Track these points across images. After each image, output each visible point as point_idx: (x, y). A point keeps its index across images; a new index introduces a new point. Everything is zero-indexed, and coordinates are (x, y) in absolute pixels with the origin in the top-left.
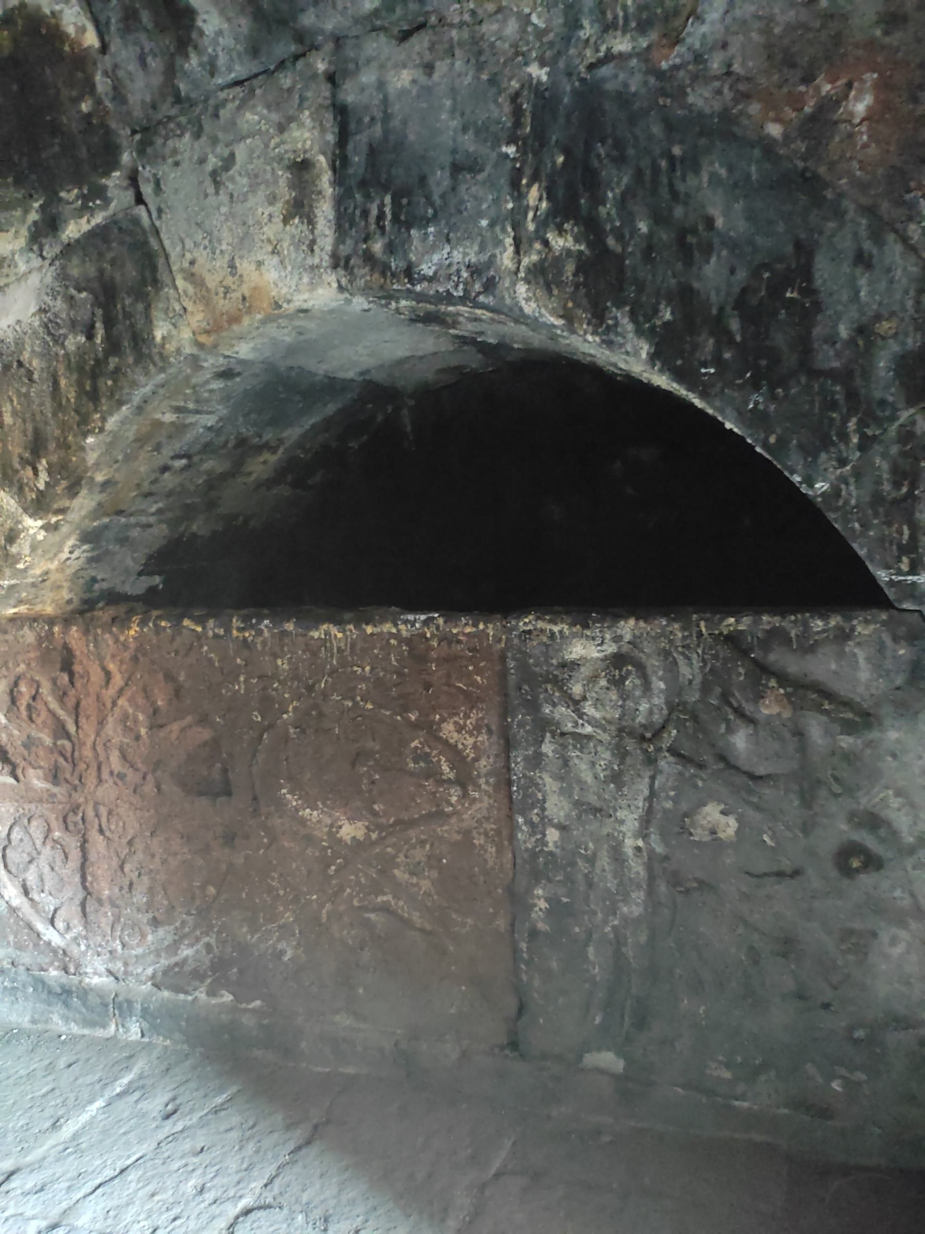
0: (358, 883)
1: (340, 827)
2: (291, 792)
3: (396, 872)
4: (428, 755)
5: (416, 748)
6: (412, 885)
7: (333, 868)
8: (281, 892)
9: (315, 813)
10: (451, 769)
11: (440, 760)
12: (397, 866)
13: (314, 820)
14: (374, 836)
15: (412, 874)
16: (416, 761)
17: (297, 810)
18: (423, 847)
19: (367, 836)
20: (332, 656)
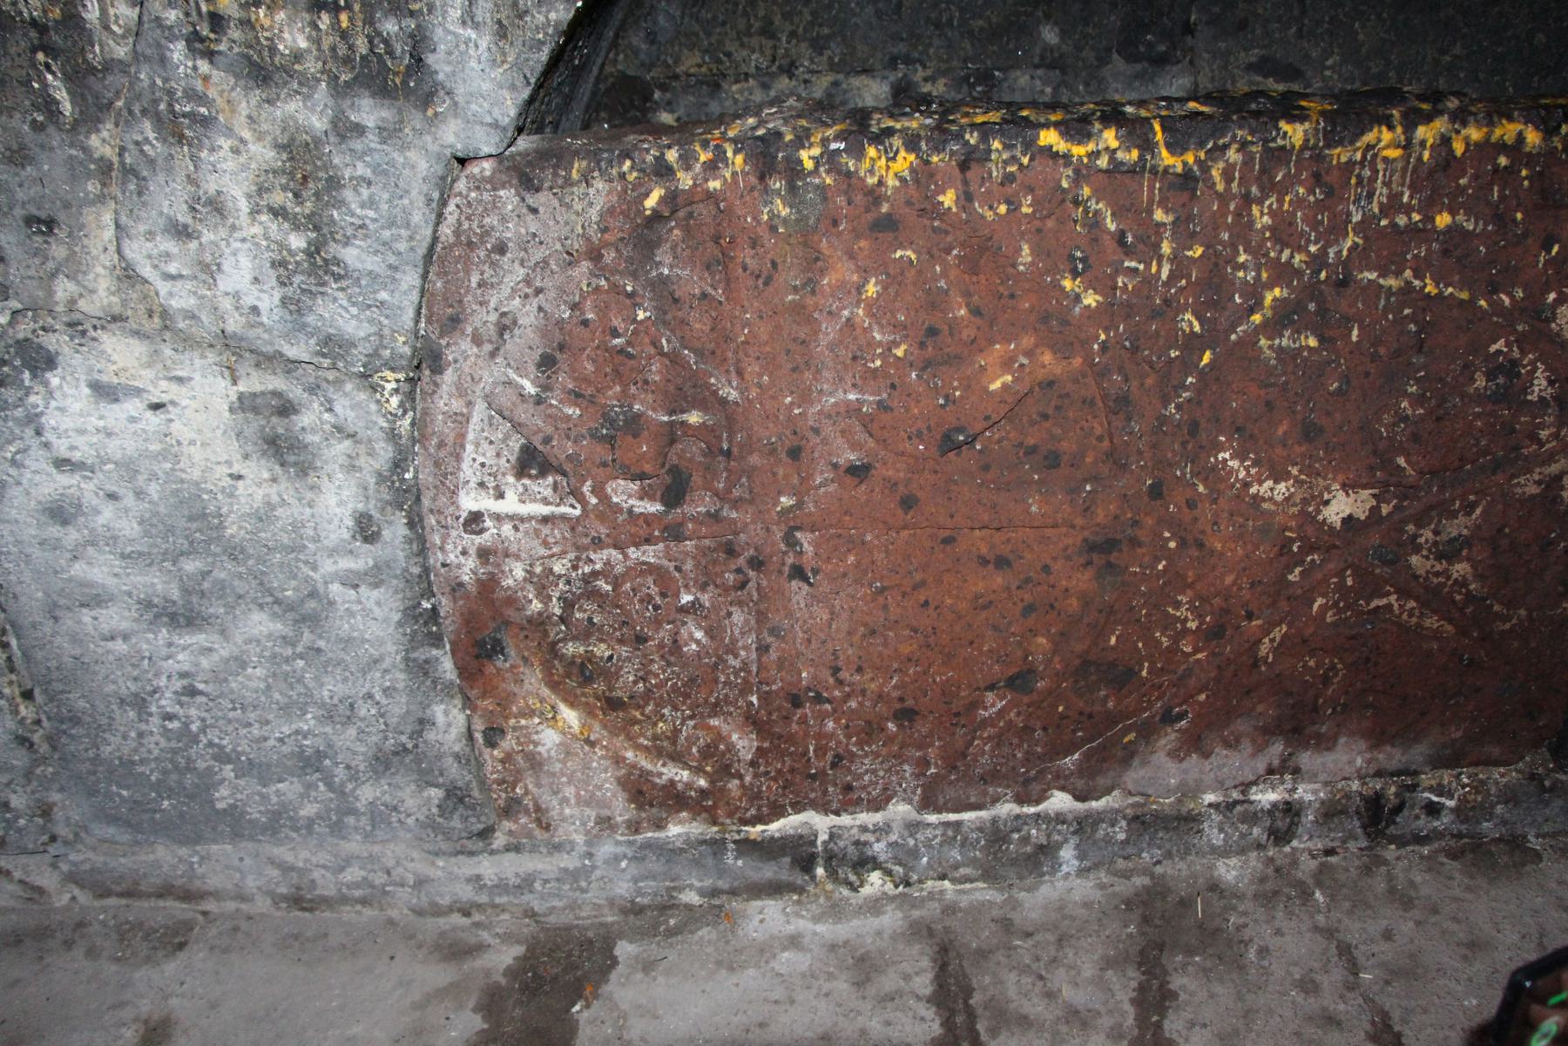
0: (1341, 585)
1: (1327, 503)
2: (1240, 455)
3: (1414, 560)
4: (1515, 363)
5: (1499, 352)
6: (1437, 574)
7: (1298, 570)
8: (1192, 625)
9: (1282, 486)
10: (1551, 383)
11: (1535, 369)
12: (1417, 549)
13: (1279, 498)
14: (1385, 510)
15: (1439, 558)
16: (1490, 376)
17: (1247, 485)
18: (1469, 514)
19: (1374, 510)
20: (1370, 195)
